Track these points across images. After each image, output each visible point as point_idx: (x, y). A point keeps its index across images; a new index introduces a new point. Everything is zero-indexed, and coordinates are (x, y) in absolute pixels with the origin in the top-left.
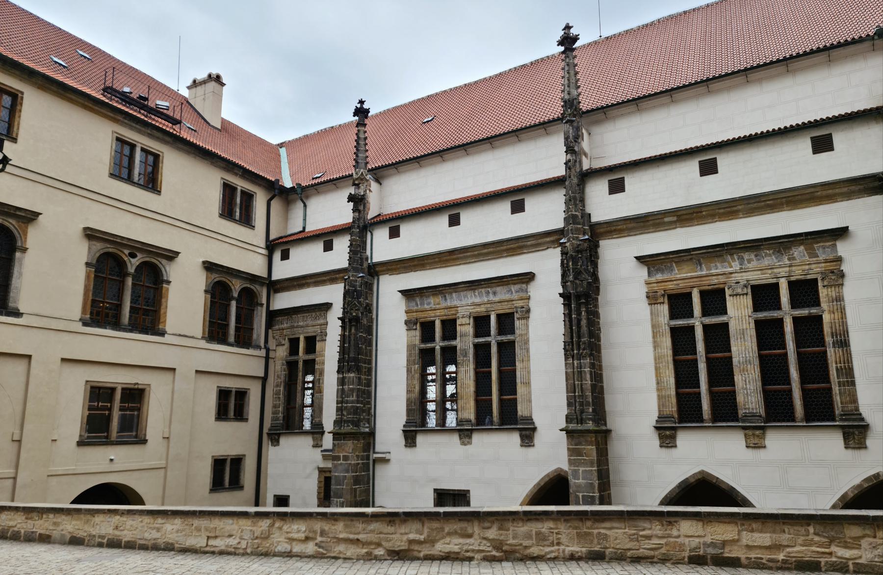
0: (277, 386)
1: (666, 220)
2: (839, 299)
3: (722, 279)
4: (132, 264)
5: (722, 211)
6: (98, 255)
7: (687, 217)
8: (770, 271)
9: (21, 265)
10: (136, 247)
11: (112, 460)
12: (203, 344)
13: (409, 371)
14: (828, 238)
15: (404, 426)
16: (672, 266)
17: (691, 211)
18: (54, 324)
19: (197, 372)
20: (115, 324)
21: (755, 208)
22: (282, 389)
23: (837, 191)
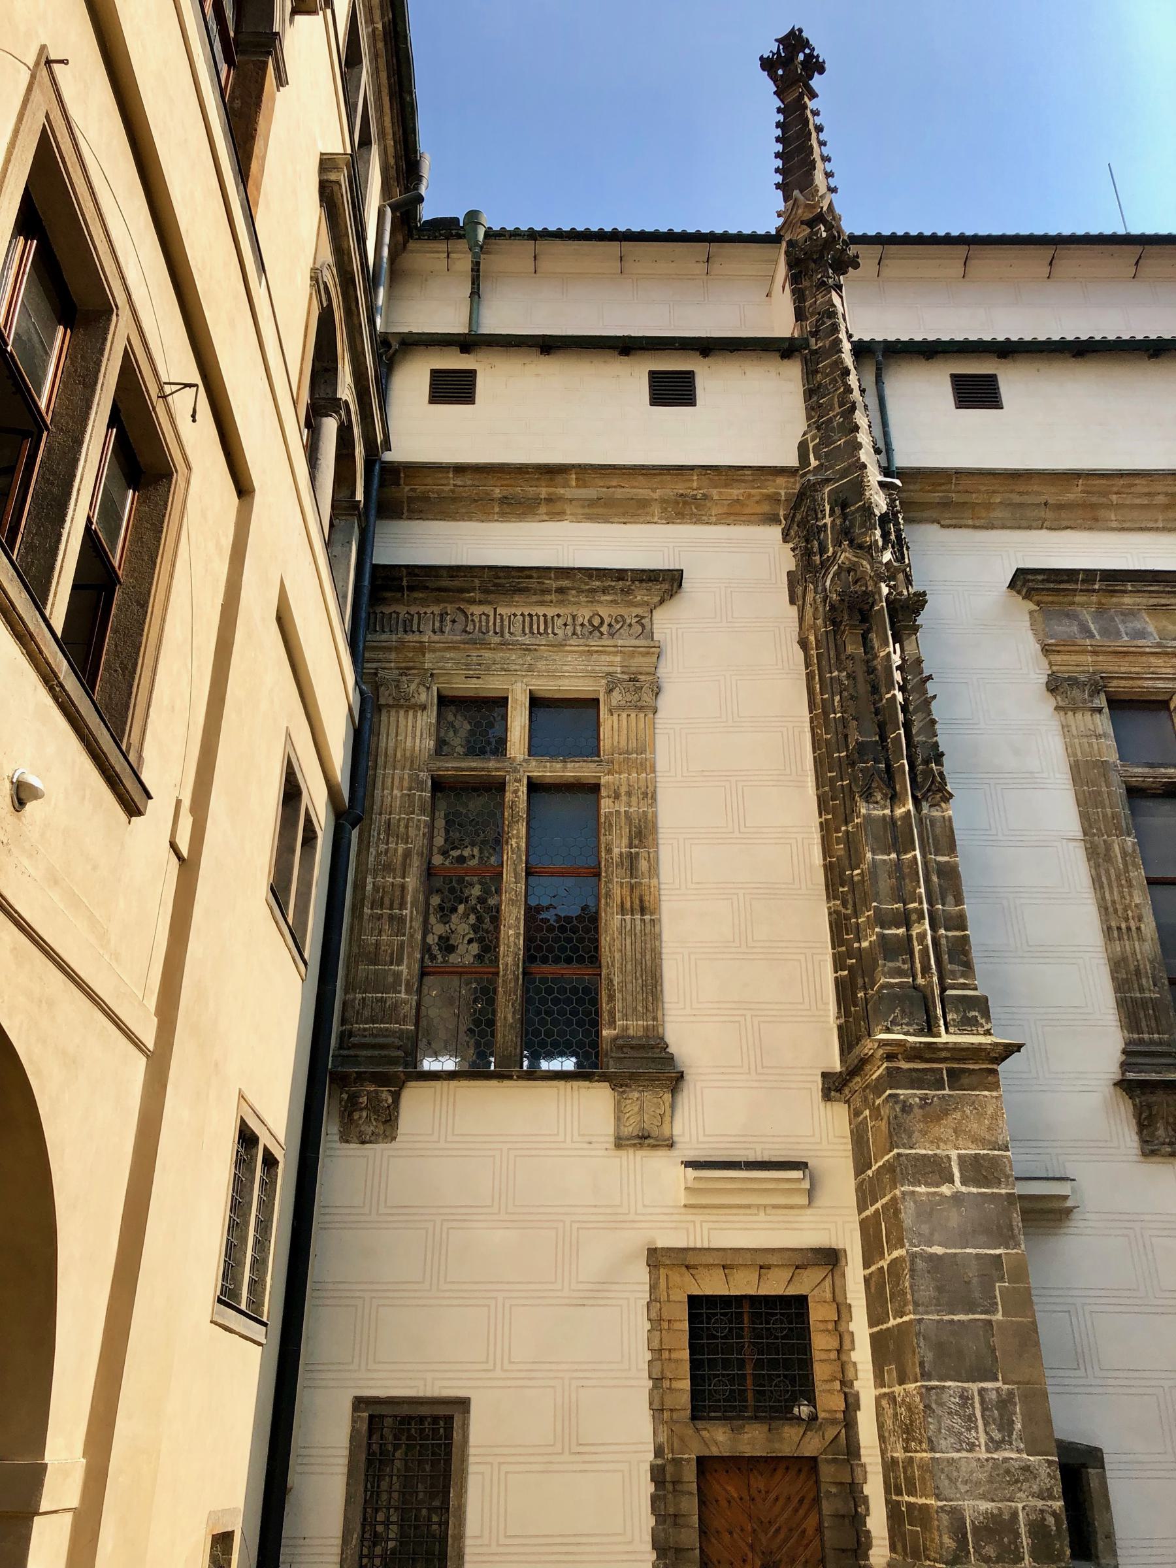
13: (1097, 855)
15: (1125, 1066)
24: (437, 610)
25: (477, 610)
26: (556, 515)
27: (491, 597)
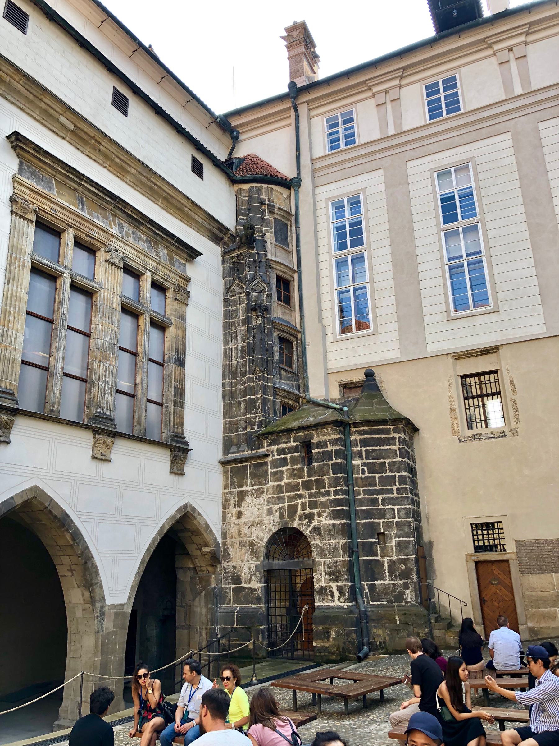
1: (62, 119)
2: (183, 318)
3: (103, 237)
5: (117, 160)
7: (85, 137)
8: (143, 257)
14: (185, 255)
16: (50, 182)
17: (92, 133)
21: (141, 182)
23: (197, 217)
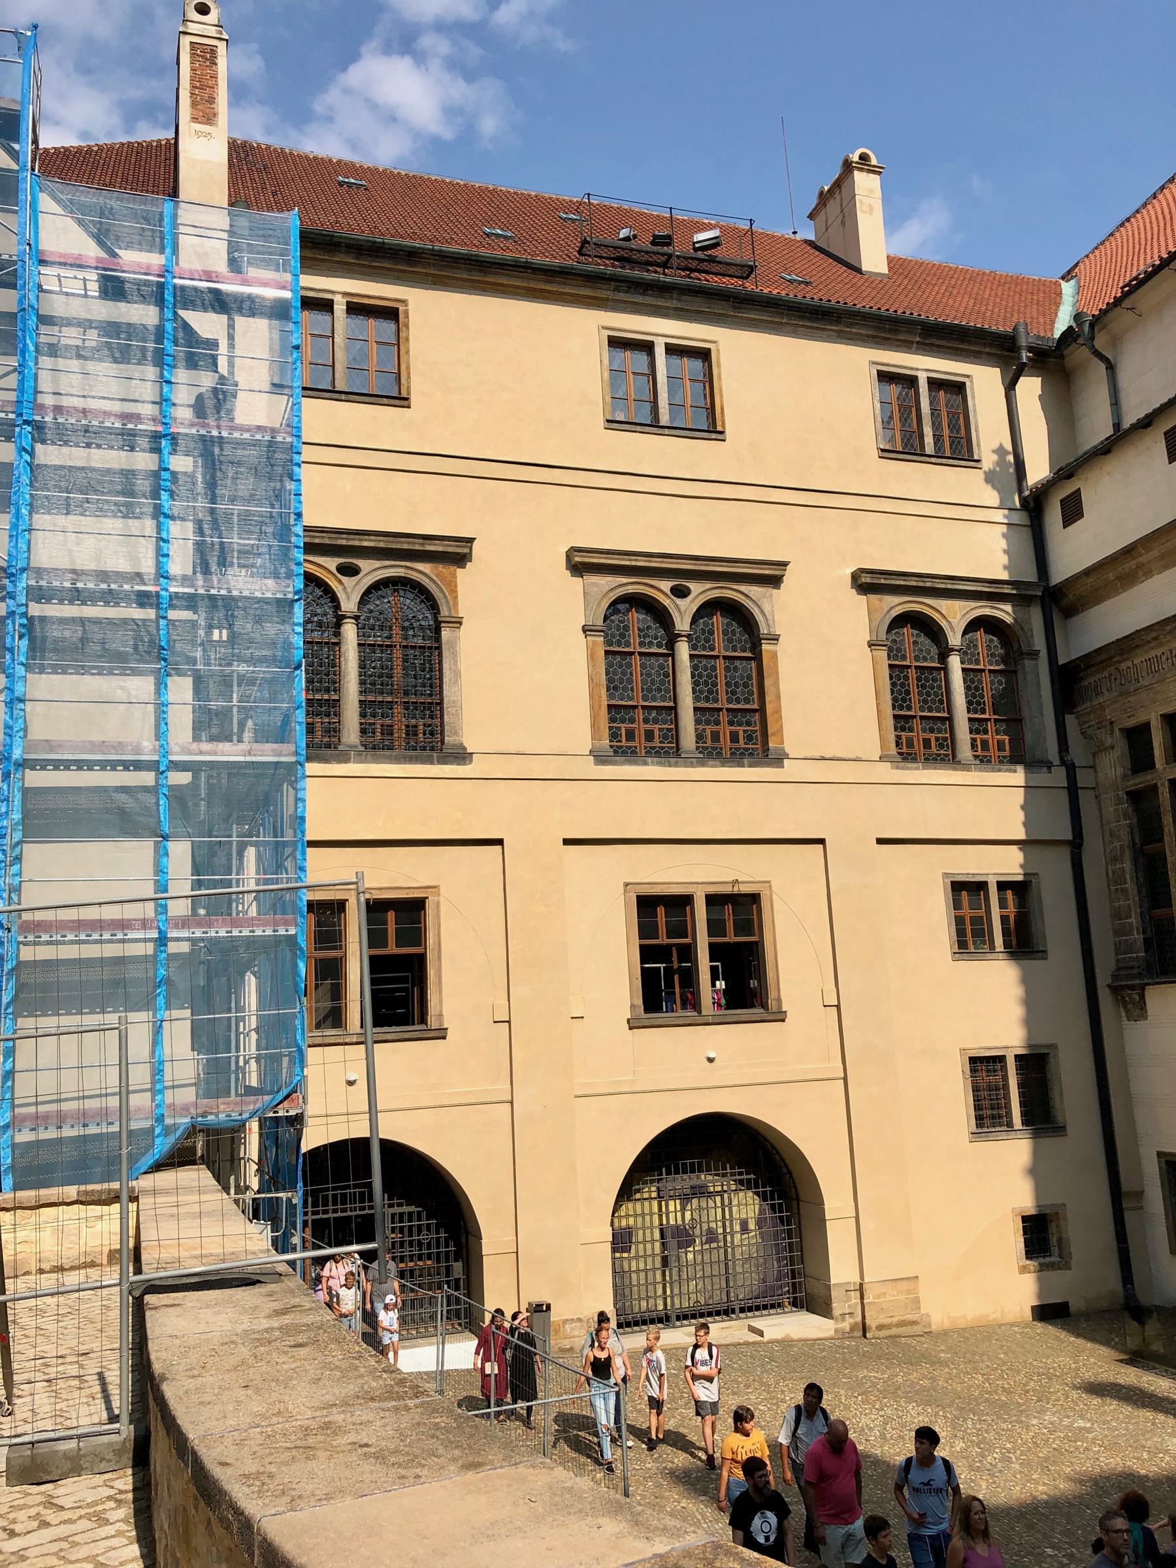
0: (1115, 860)
4: (683, 613)
6: (605, 604)
9: (455, 655)
10: (683, 572)
11: (711, 1060)
12: (886, 772)
18: (536, 768)
19: (880, 841)
20: (667, 749)
22: (1127, 865)
24: (1106, 674)
25: (1123, 666)
26: (1149, 574)
27: (1126, 656)
